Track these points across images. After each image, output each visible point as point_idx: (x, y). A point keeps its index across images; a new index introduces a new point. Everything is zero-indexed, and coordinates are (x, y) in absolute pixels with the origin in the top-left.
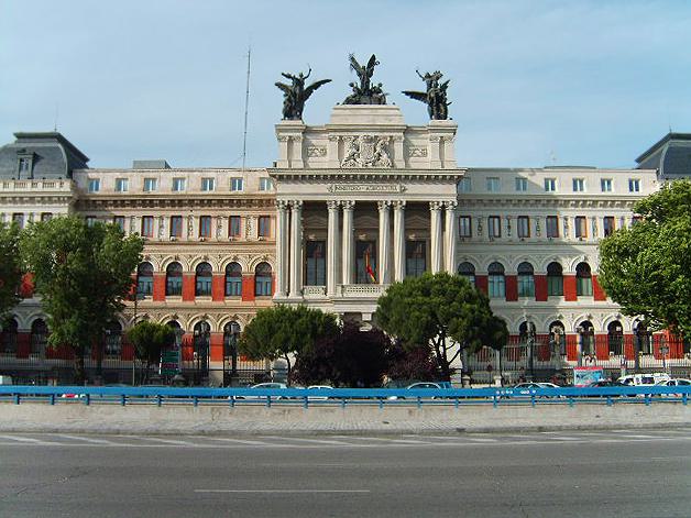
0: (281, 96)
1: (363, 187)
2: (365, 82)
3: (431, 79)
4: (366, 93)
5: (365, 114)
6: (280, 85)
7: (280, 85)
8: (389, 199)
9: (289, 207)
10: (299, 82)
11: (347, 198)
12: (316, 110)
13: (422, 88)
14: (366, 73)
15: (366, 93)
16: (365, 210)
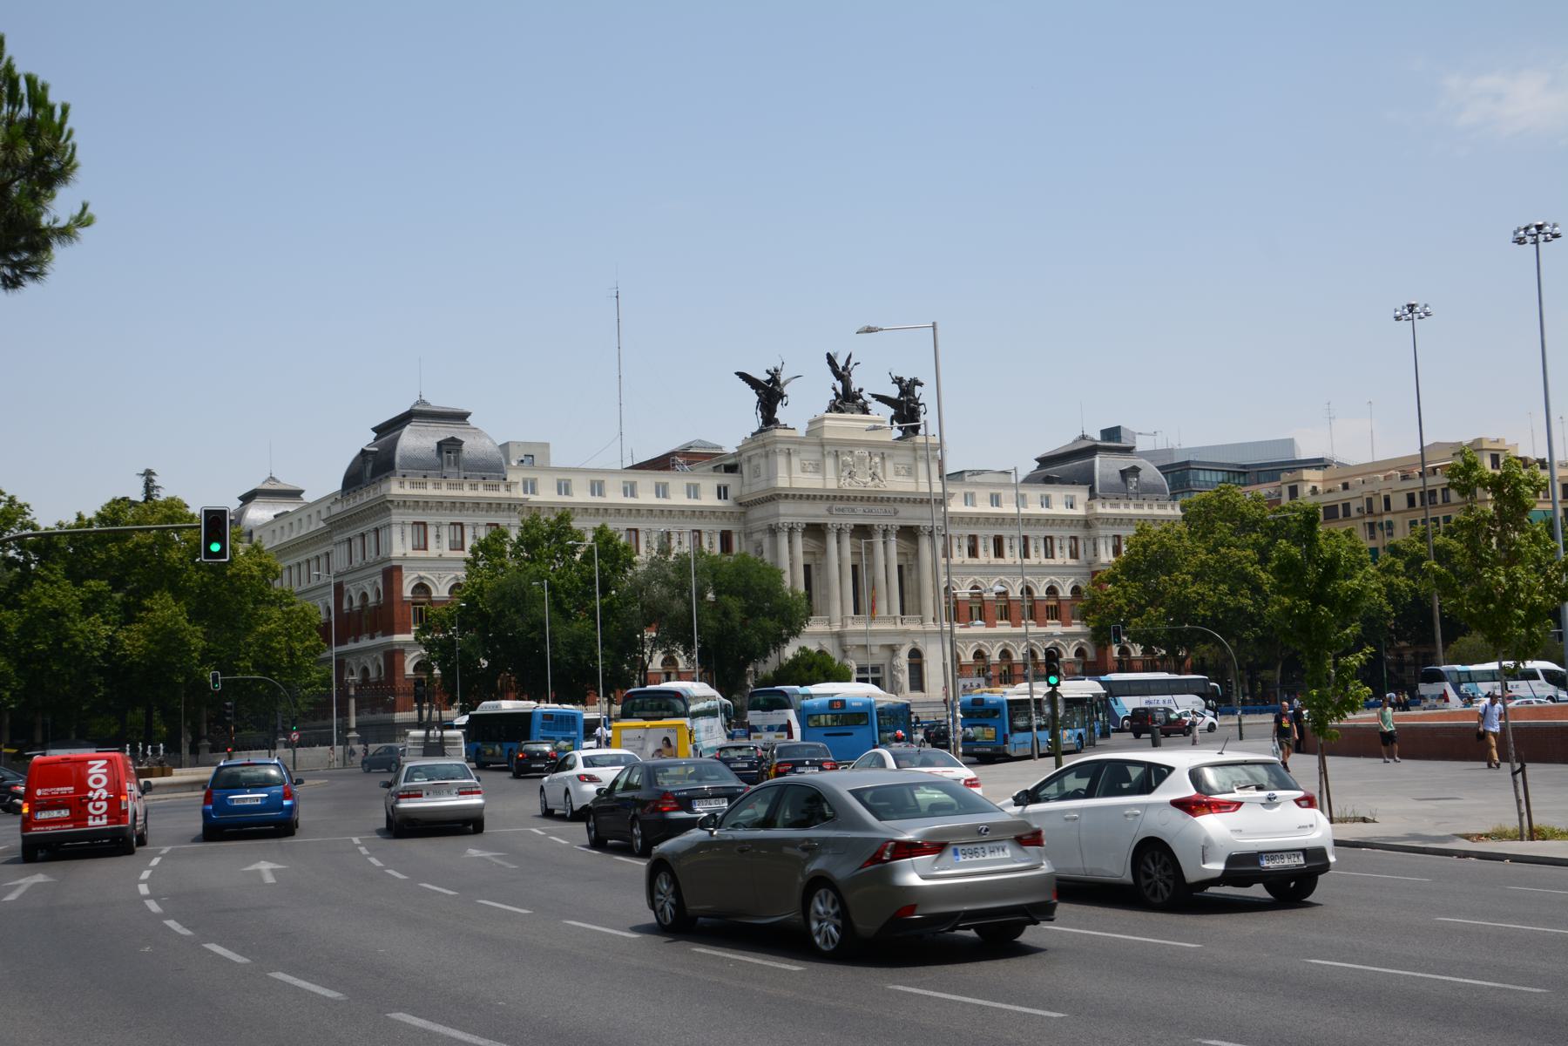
0: (752, 397)
1: (860, 508)
2: (846, 387)
3: (908, 388)
4: (847, 400)
5: (847, 425)
6: (744, 377)
7: (744, 377)
8: (884, 522)
9: (791, 530)
10: (774, 378)
11: (844, 521)
12: (793, 415)
13: (894, 392)
14: (842, 375)
15: (847, 400)
16: (862, 531)
